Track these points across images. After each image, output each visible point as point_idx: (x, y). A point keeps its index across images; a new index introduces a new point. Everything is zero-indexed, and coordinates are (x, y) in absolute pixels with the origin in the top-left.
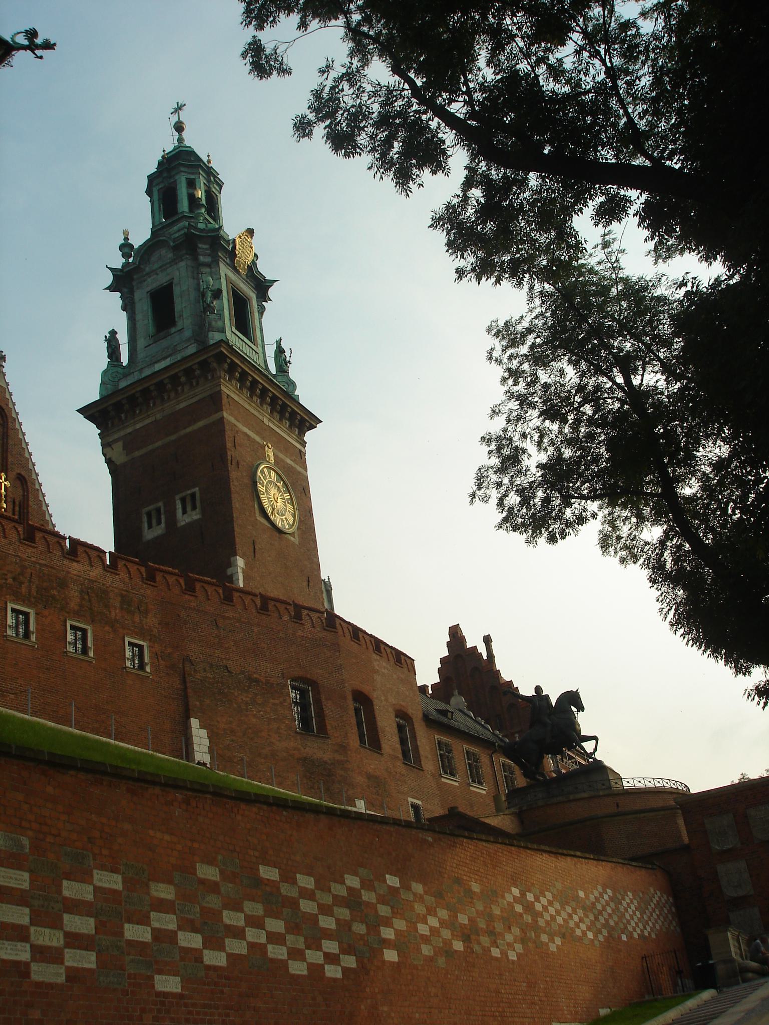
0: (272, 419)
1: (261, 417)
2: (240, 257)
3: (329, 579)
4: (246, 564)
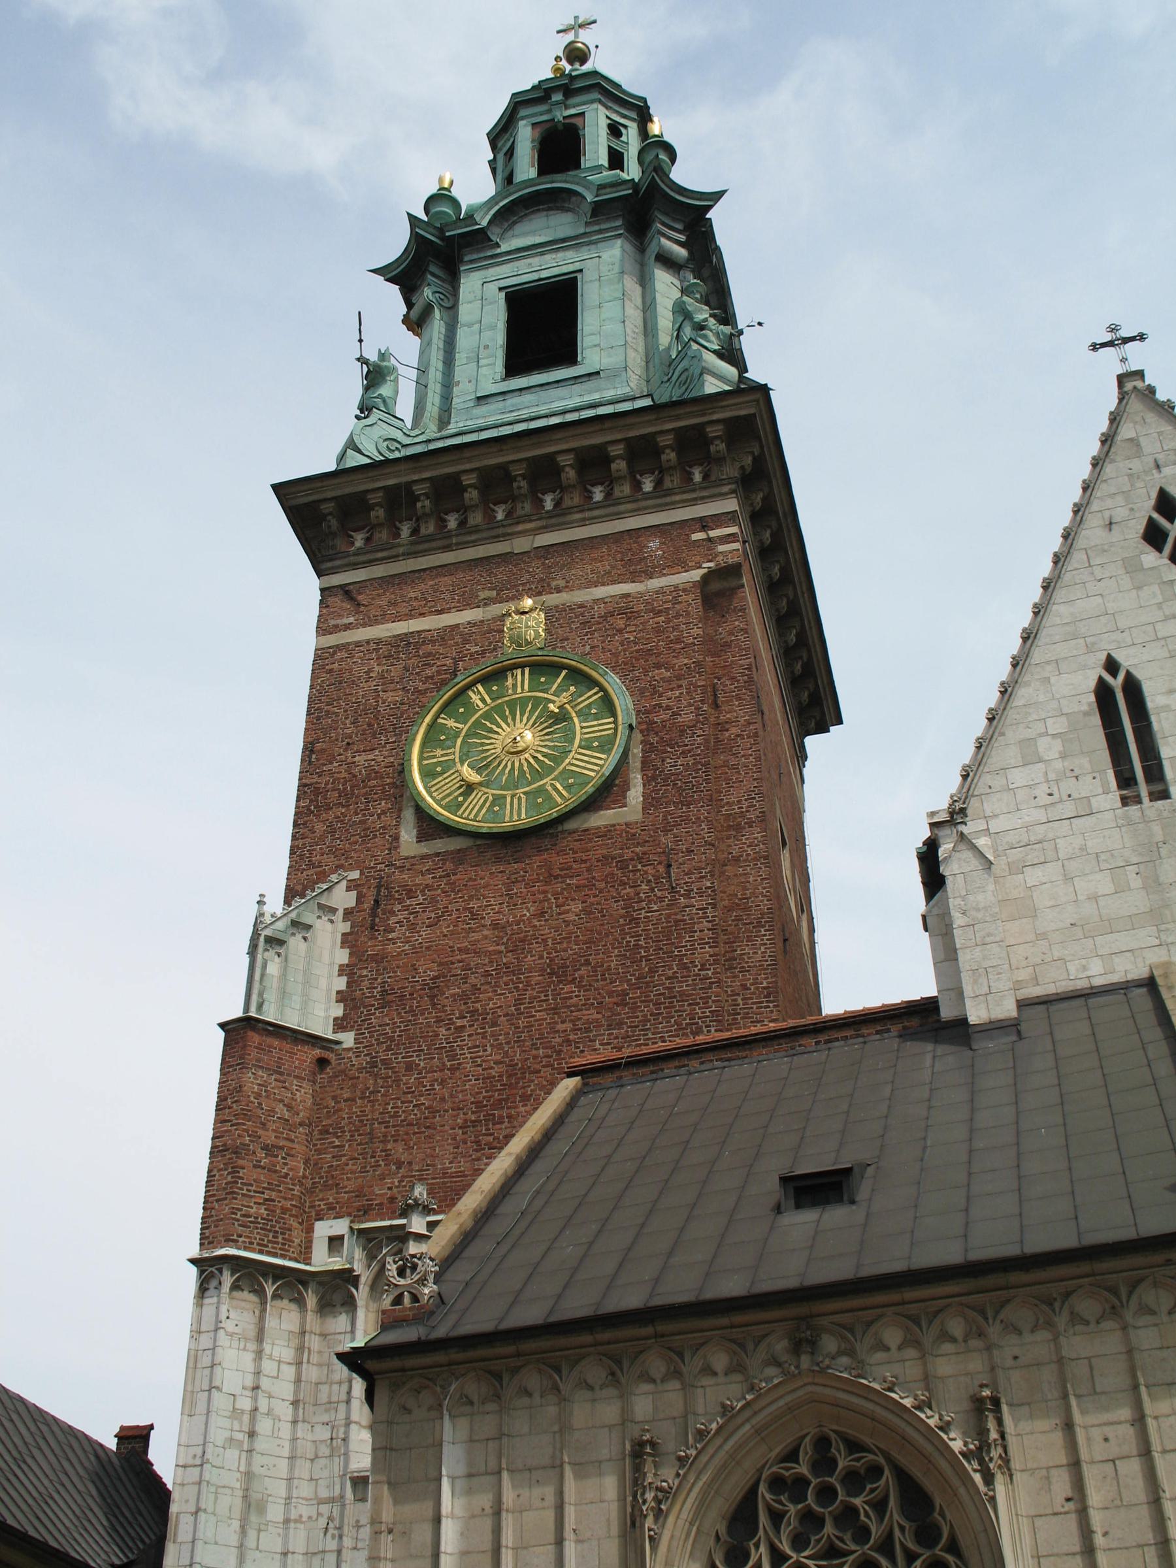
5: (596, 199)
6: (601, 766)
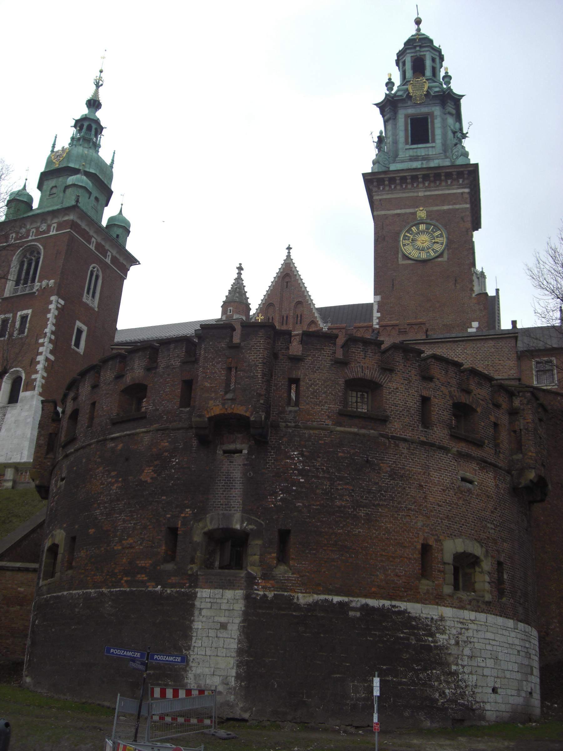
0: (428, 189)
1: (415, 194)
2: (415, 95)
3: (482, 269)
4: (382, 298)
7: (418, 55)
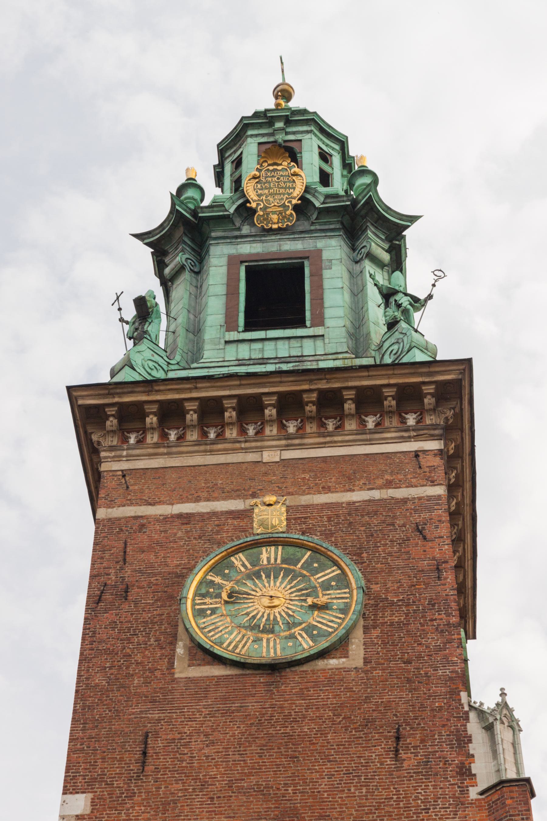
0: (297, 441)
1: (251, 457)
2: (265, 208)
3: (503, 694)
5: (321, 206)
6: (340, 625)
7: (280, 140)
